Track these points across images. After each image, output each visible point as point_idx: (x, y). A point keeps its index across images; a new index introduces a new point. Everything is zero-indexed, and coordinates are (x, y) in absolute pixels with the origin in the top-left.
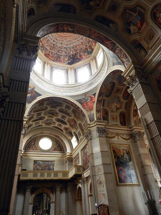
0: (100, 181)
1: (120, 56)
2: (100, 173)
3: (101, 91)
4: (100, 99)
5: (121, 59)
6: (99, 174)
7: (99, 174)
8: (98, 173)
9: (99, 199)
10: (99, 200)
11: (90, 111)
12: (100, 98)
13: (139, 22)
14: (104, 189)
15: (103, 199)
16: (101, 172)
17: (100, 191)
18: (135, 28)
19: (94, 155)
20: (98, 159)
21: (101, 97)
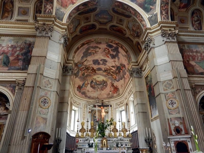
0: (45, 99)
1: (163, 7)
2: (49, 89)
3: (90, 3)
4: (80, 8)
5: (162, 9)
6: (45, 88)
7: (45, 88)
8: (45, 87)
9: (35, 123)
10: (34, 125)
11: (62, 6)
12: (81, 7)
13: (184, 4)
14: (48, 112)
15: (42, 125)
16: (51, 87)
17: (40, 112)
18: (179, 3)
19: (47, 62)
20: (51, 70)
21: (83, 7)
